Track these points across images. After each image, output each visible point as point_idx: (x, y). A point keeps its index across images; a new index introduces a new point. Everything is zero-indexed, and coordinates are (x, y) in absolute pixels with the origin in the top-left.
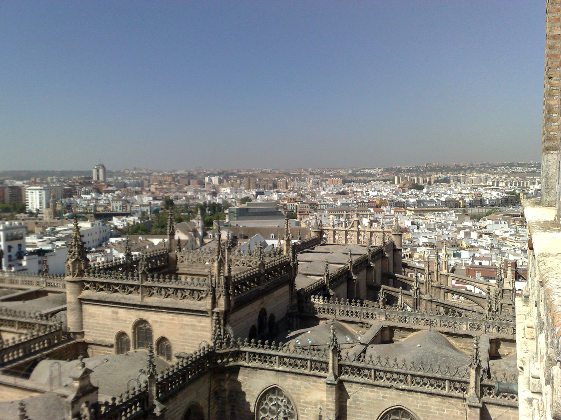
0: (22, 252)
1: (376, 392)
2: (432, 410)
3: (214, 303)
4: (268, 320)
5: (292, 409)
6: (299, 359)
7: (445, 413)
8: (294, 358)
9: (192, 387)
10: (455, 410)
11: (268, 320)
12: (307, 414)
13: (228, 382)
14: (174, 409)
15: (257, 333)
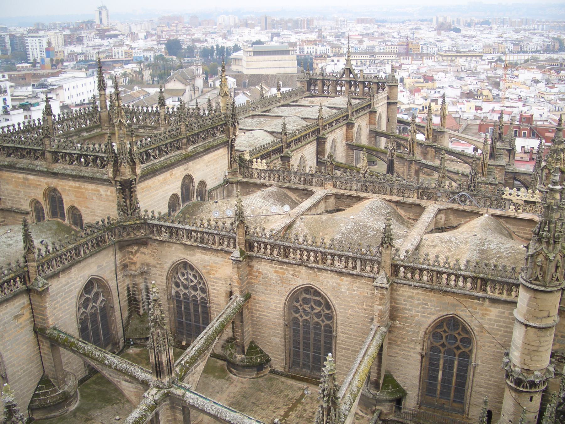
0: (8, 106)
1: (286, 269)
2: (342, 290)
3: (116, 171)
4: (196, 187)
5: (204, 284)
6: (207, 233)
7: (355, 292)
8: (202, 232)
9: (91, 260)
10: (365, 290)
11: (196, 187)
12: (218, 290)
13: (138, 255)
14: (68, 283)
15: (180, 202)
